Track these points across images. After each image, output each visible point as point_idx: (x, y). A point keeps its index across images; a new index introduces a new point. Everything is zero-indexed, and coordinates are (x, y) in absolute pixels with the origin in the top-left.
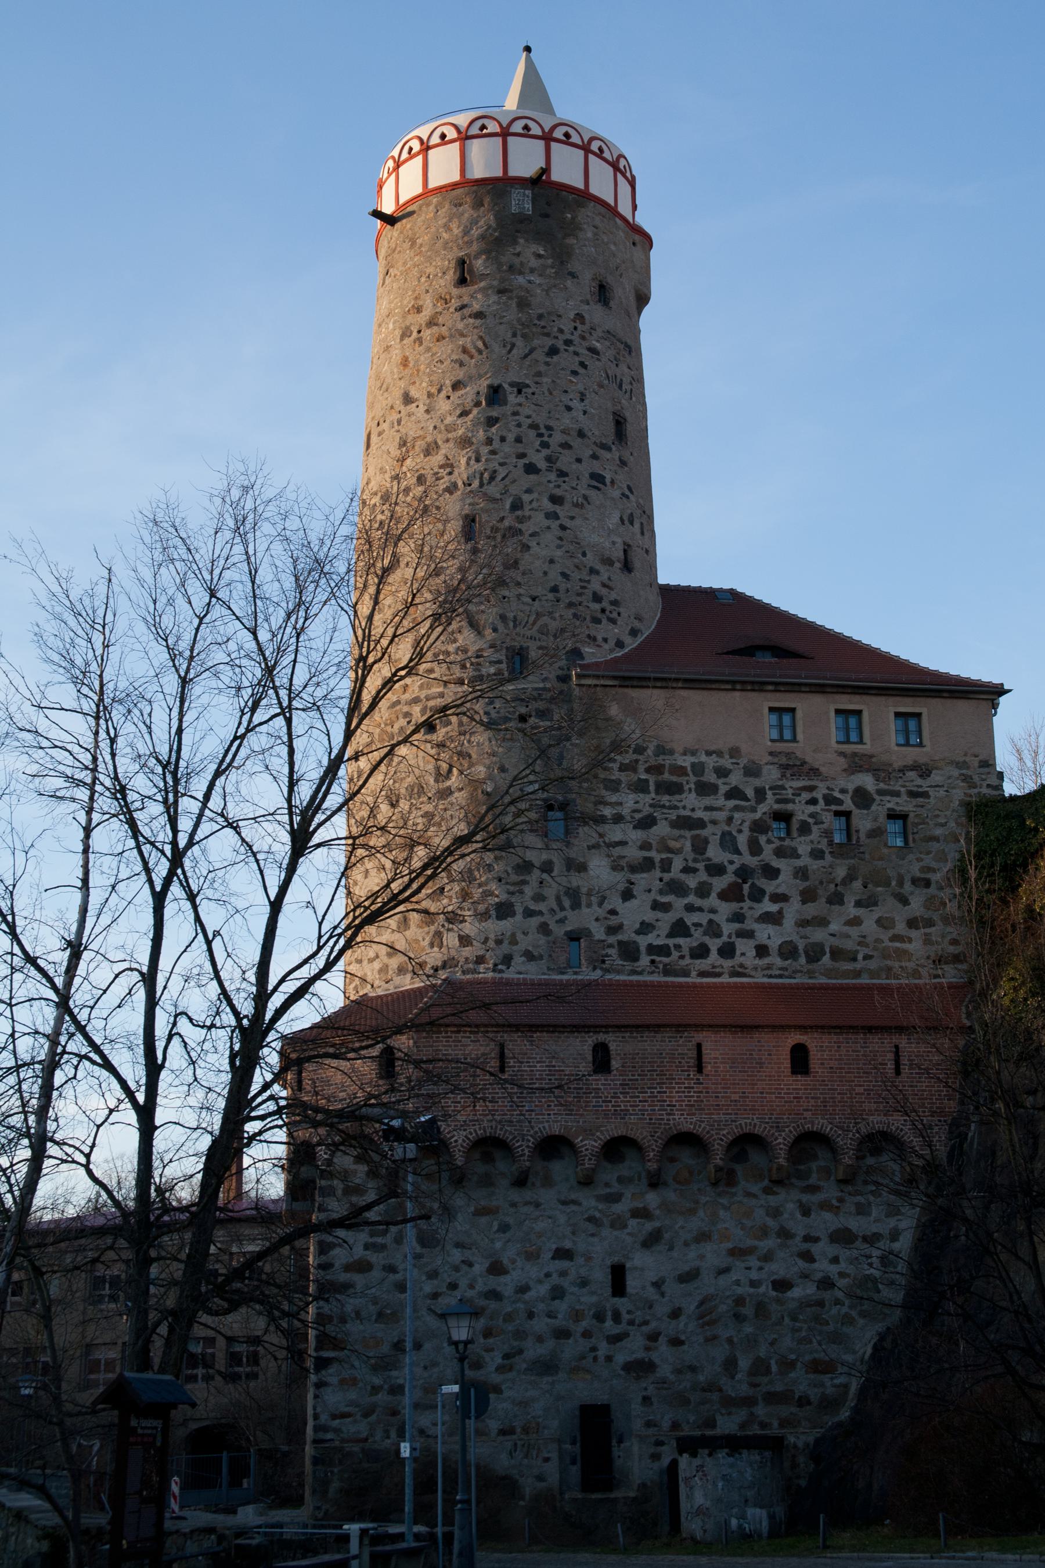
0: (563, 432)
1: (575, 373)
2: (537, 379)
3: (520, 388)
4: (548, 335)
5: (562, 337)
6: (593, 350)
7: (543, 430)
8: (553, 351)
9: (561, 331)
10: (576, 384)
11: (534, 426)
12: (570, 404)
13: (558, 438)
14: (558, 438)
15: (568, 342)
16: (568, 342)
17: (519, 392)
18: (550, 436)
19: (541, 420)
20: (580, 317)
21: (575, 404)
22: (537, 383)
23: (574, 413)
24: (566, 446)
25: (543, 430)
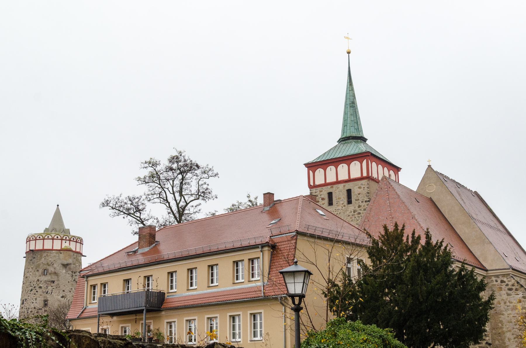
0: (31, 309)
1: (35, 294)
2: (28, 297)
3: (26, 299)
4: (31, 286)
5: (34, 286)
6: (40, 287)
7: (28, 309)
8: (32, 290)
9: (34, 285)
10: (35, 296)
11: (26, 309)
12: (33, 302)
13: (30, 310)
14: (30, 310)
15: (35, 287)
16: (35, 287)
17: (26, 301)
18: (29, 310)
19: (28, 307)
20: (38, 280)
21: (35, 301)
22: (28, 298)
23: (34, 303)
24: (31, 312)
25: (28, 309)
